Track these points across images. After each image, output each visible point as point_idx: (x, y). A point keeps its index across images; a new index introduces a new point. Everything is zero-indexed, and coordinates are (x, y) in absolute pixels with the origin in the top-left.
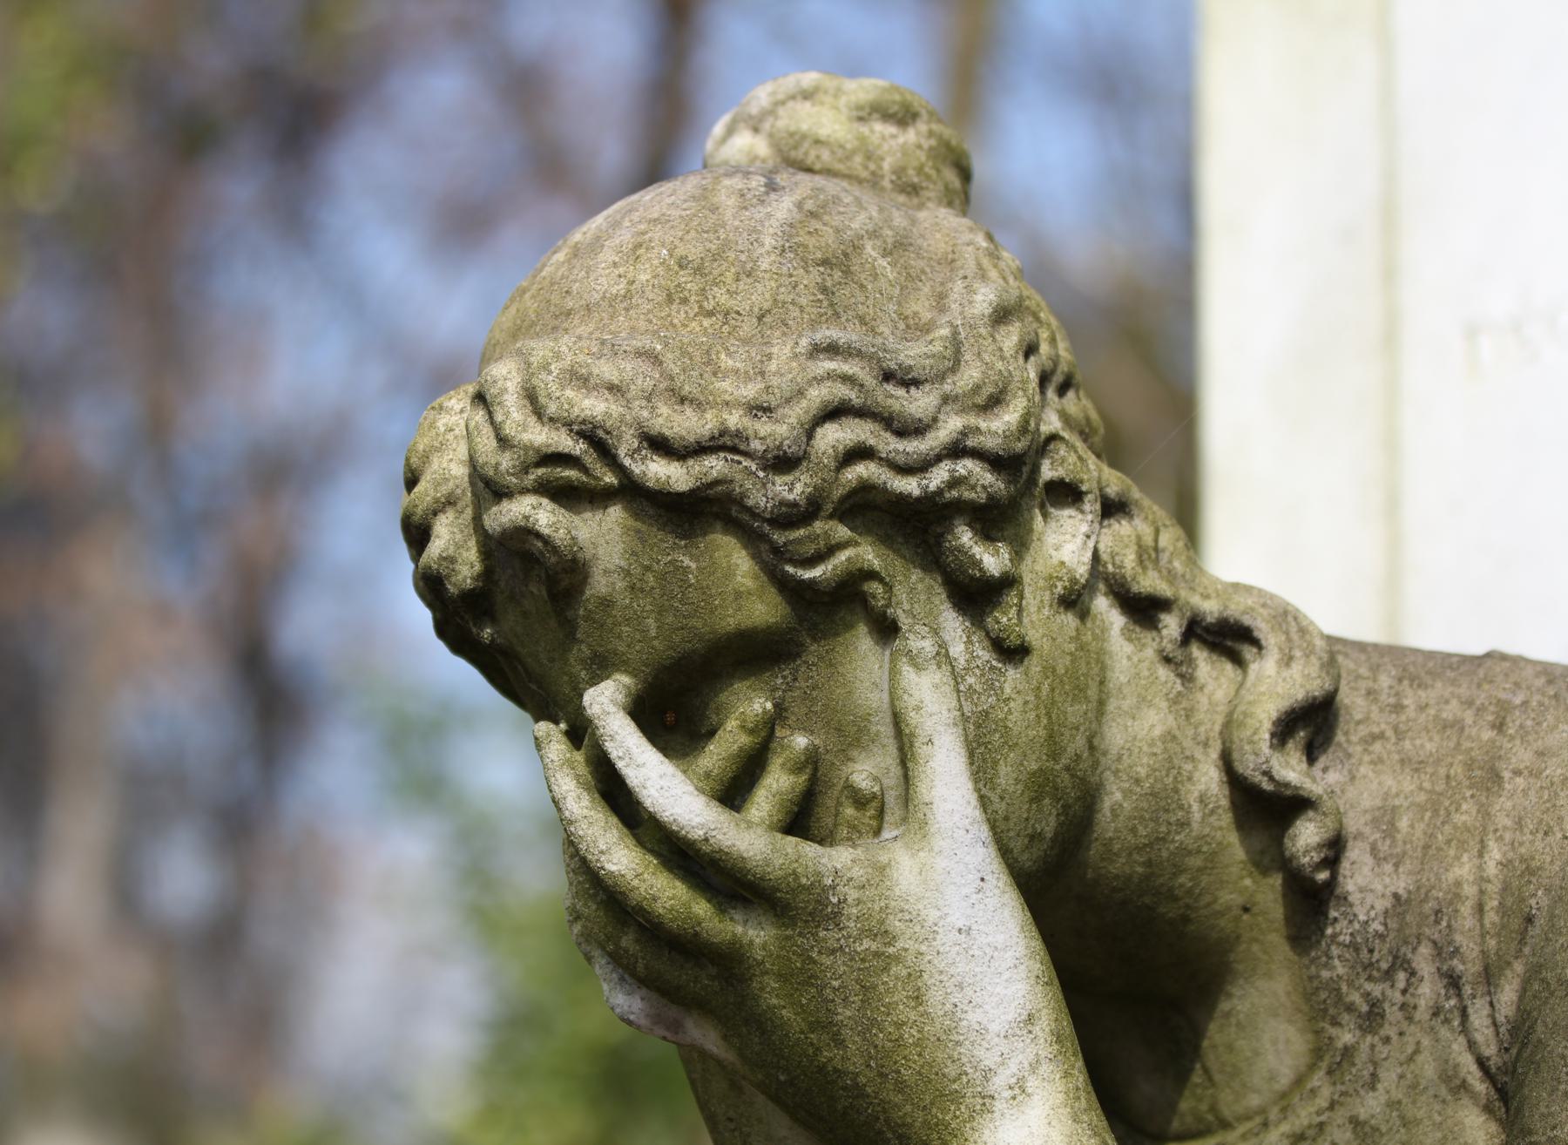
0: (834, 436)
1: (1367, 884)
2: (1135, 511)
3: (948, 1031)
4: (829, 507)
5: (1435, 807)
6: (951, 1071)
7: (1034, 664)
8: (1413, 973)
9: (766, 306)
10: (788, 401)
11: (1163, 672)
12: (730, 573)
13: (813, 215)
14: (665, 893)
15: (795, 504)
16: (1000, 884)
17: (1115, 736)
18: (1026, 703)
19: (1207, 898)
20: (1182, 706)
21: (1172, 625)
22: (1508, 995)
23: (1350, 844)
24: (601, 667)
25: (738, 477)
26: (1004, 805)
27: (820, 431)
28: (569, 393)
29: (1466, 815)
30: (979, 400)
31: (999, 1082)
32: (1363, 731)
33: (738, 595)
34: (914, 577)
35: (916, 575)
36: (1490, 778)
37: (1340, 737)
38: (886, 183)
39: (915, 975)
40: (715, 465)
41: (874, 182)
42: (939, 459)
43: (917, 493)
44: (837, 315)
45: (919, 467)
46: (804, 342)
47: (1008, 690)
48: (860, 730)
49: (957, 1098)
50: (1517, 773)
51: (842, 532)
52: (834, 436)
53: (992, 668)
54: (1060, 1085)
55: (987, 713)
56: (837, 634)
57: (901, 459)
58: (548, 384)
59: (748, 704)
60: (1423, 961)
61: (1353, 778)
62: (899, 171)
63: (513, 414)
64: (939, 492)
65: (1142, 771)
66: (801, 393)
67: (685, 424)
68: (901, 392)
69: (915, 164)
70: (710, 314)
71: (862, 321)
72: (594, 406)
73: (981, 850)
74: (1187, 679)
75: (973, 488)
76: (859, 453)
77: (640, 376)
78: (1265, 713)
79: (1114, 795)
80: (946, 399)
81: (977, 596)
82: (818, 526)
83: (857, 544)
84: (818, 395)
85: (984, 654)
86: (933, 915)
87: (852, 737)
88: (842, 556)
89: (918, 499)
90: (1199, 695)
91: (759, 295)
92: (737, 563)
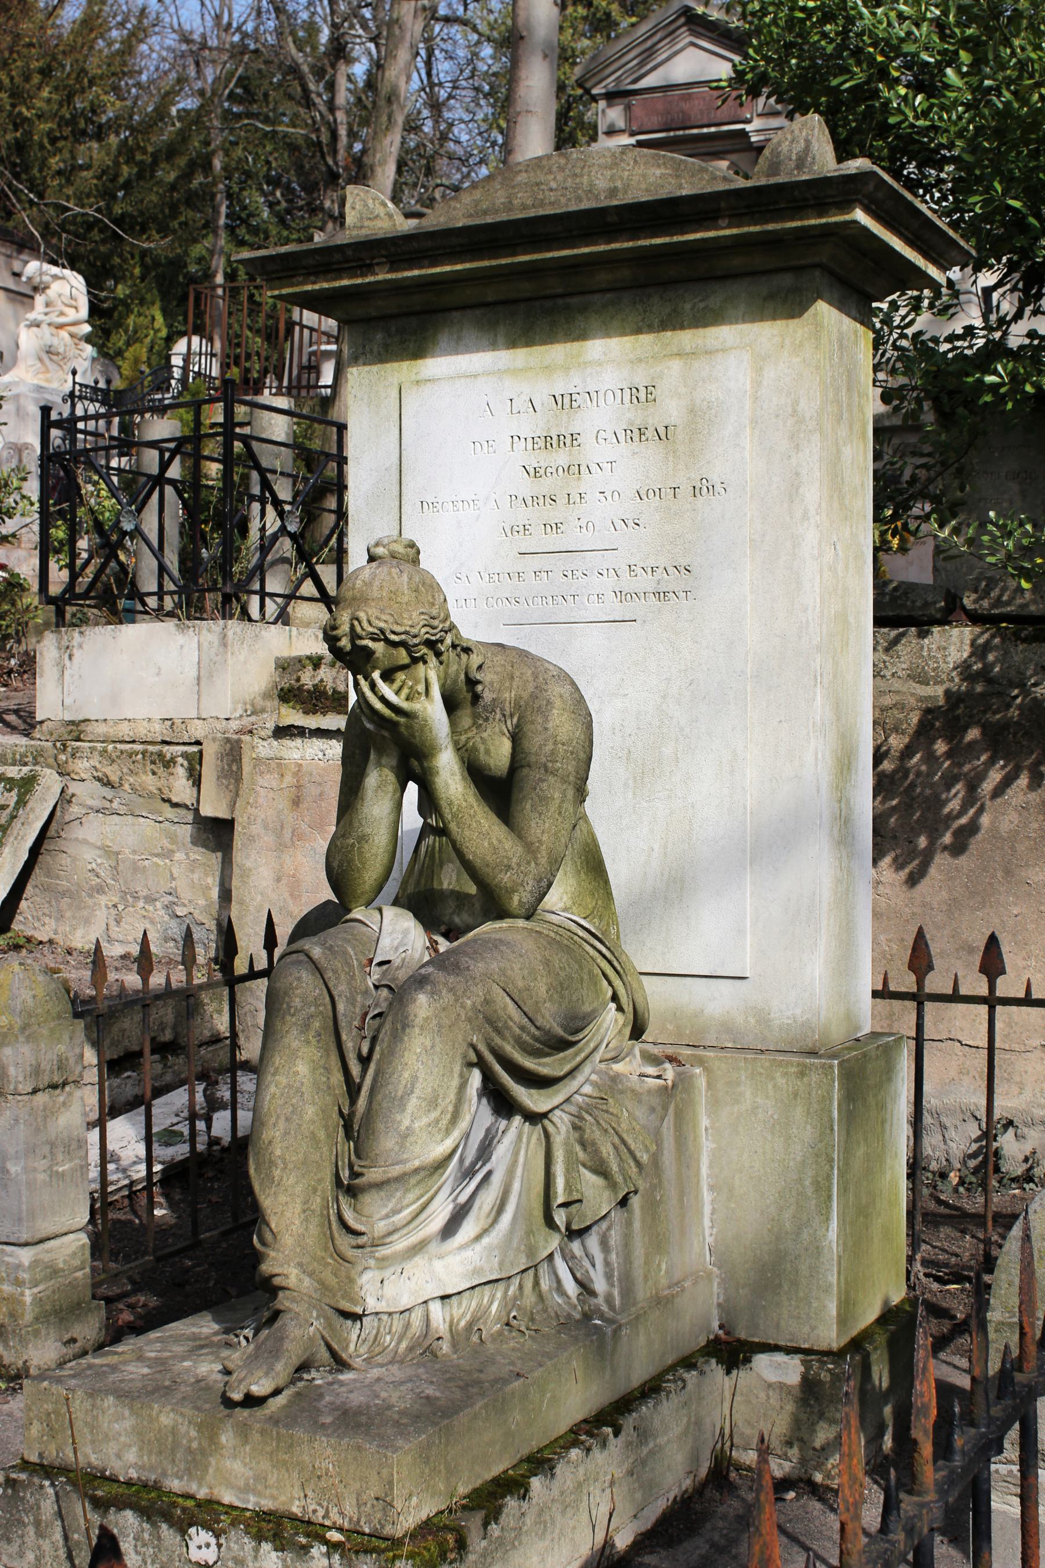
0: (424, 630)
1: (488, 696)
5: (502, 682)
14: (387, 712)
20: (459, 664)
22: (515, 720)
24: (374, 668)
29: (507, 684)
36: (512, 678)
40: (403, 637)
52: (424, 630)
58: (373, 619)
59: (401, 676)
60: (498, 711)
63: (365, 625)
72: (382, 625)
77: (391, 620)
78: (475, 666)
81: (438, 654)
87: (417, 682)
91: (406, 599)
92: (403, 652)
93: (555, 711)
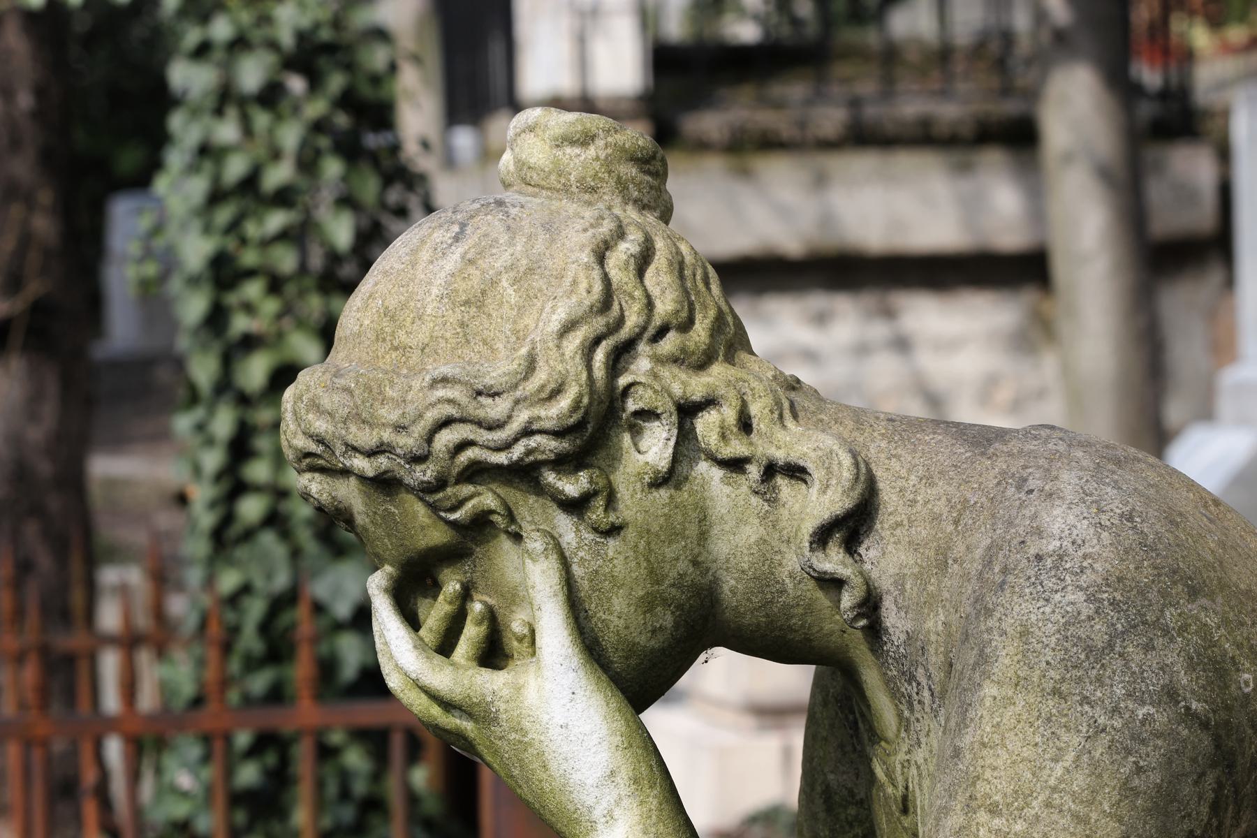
0: (446, 438)
2: (722, 402)
3: (564, 786)
4: (453, 480)
6: (571, 807)
7: (630, 534)
8: (919, 684)
9: (426, 341)
10: (414, 422)
11: (755, 500)
12: (415, 516)
13: (472, 262)
15: (429, 482)
16: (588, 693)
17: (721, 547)
18: (626, 558)
19: (816, 629)
21: (754, 471)
23: (884, 597)
25: (396, 468)
26: (622, 621)
27: (437, 436)
28: (310, 416)
30: (543, 395)
31: (598, 813)
32: (892, 520)
33: (423, 528)
34: (531, 501)
35: (532, 499)
37: (878, 526)
38: (574, 189)
39: (540, 754)
40: (383, 462)
41: (566, 189)
42: (516, 440)
43: (506, 462)
44: (468, 341)
45: (507, 446)
46: (428, 378)
47: (611, 554)
48: (513, 595)
49: (578, 822)
50: (955, 561)
51: (467, 489)
52: (446, 438)
53: (597, 543)
54: (636, 811)
55: (597, 572)
56: (488, 542)
57: (492, 444)
61: (884, 554)
62: (581, 180)
64: (521, 459)
65: (746, 566)
66: (421, 416)
67: (366, 438)
68: (490, 400)
69: (592, 172)
70: (396, 349)
71: (485, 342)
73: (572, 675)
74: (773, 501)
75: (543, 452)
79: (730, 585)
80: (517, 402)
82: (449, 491)
83: (480, 494)
84: (431, 416)
85: (589, 536)
86: (546, 718)
88: (469, 505)
89: (508, 466)
90: (782, 510)
91: (422, 335)
93: (990, 690)
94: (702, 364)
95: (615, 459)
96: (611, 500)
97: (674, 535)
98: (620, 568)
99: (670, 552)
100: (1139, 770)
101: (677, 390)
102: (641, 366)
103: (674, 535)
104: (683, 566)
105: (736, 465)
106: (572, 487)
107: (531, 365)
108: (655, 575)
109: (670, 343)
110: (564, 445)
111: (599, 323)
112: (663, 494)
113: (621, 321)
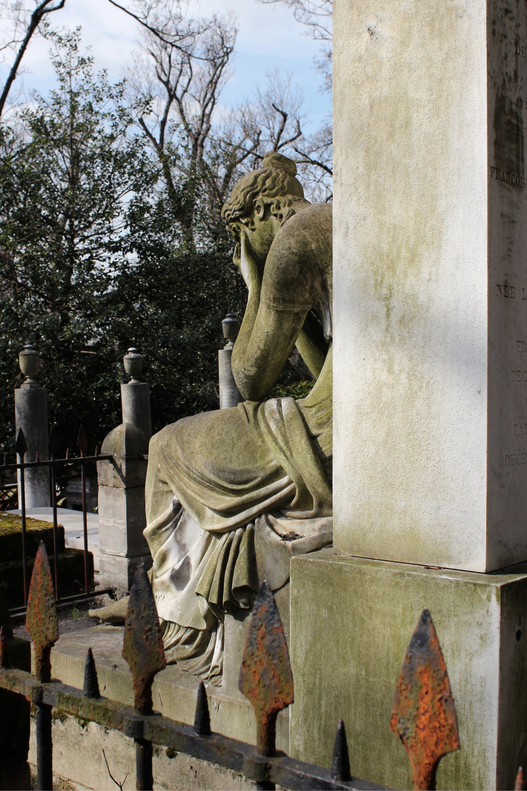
7: (257, 230)
76: (229, 215)
94: (274, 196)
95: (254, 216)
96: (253, 223)
97: (265, 230)
98: (256, 237)
99: (265, 234)
100: (281, 264)
101: (265, 201)
102: (260, 197)
103: (265, 230)
104: (267, 236)
105: (276, 215)
106: (244, 221)
107: (237, 198)
108: (262, 239)
109: (266, 193)
110: (240, 213)
111: (249, 189)
112: (263, 222)
113: (257, 187)
